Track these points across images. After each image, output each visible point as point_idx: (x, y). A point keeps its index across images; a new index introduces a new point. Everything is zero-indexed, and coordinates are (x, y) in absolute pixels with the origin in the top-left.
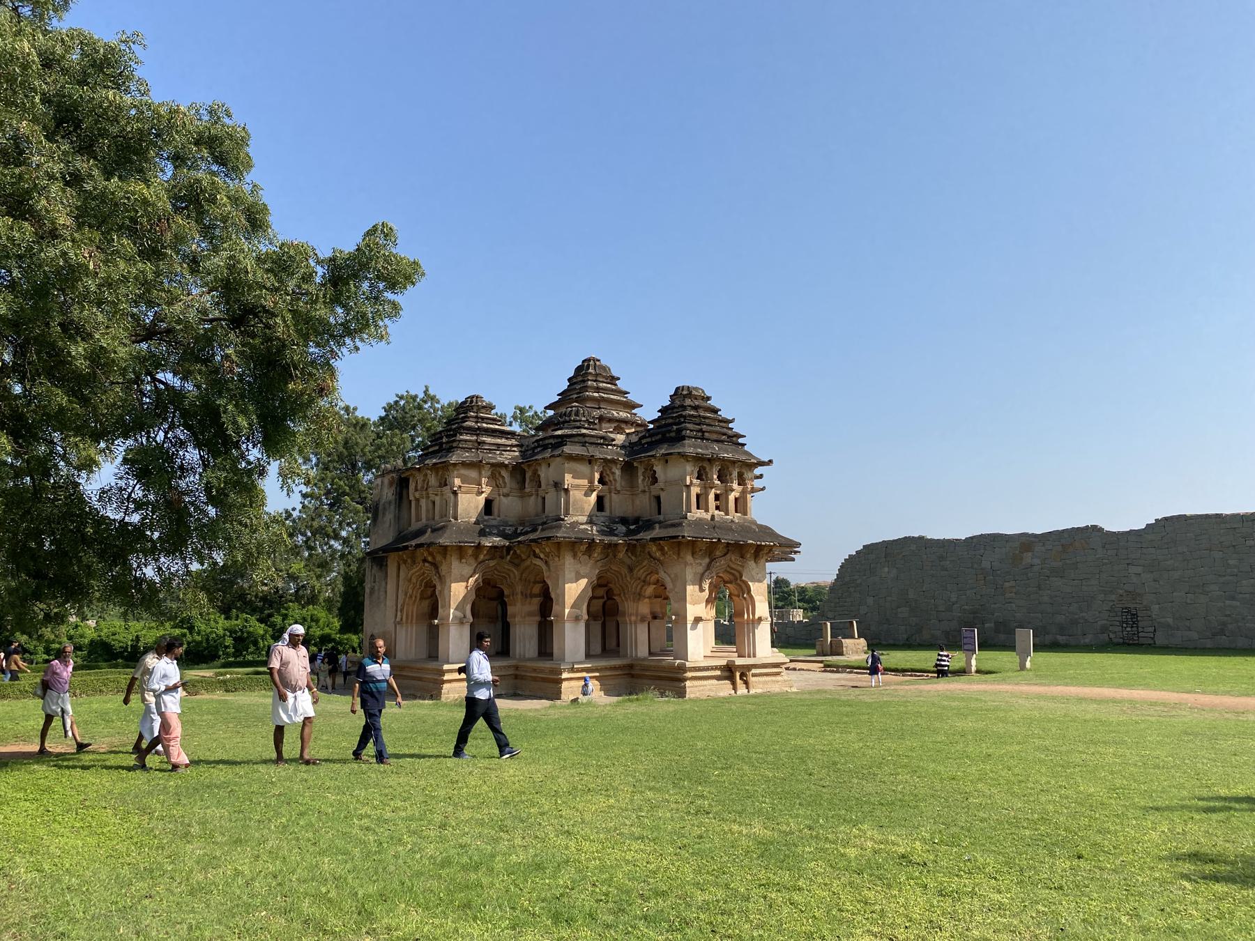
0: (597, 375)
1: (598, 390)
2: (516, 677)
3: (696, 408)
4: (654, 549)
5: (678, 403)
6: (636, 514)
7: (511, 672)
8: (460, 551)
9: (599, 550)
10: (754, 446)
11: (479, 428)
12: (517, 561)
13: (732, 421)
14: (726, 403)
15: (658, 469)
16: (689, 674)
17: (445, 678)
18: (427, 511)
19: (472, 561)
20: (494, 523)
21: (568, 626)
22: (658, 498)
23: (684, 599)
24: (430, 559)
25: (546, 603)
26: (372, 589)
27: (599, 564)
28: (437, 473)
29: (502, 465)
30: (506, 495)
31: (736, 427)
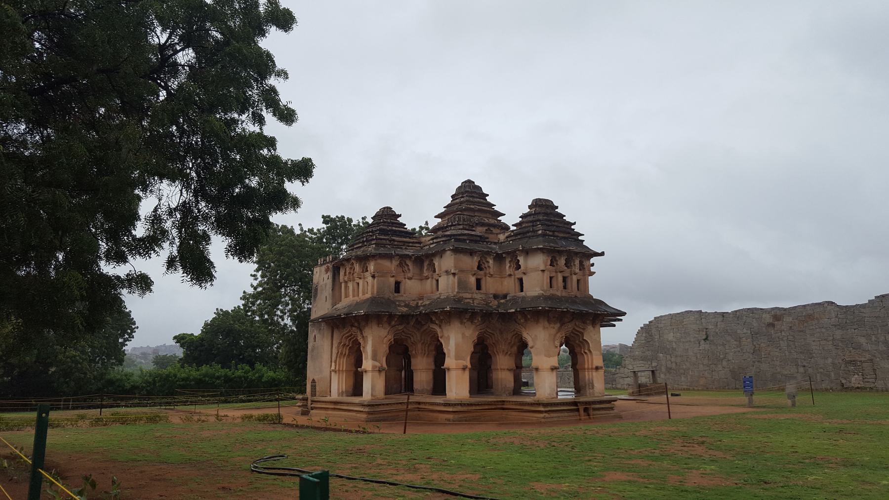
0: (472, 192)
1: (474, 203)
2: (419, 409)
3: (546, 214)
10: (590, 242)
11: (390, 231)
13: (575, 223)
15: (521, 259)
18: (353, 290)
19: (386, 325)
20: (401, 299)
22: (521, 280)
24: (356, 324)
25: (439, 356)
29: (407, 256)
30: (410, 279)
31: (576, 228)
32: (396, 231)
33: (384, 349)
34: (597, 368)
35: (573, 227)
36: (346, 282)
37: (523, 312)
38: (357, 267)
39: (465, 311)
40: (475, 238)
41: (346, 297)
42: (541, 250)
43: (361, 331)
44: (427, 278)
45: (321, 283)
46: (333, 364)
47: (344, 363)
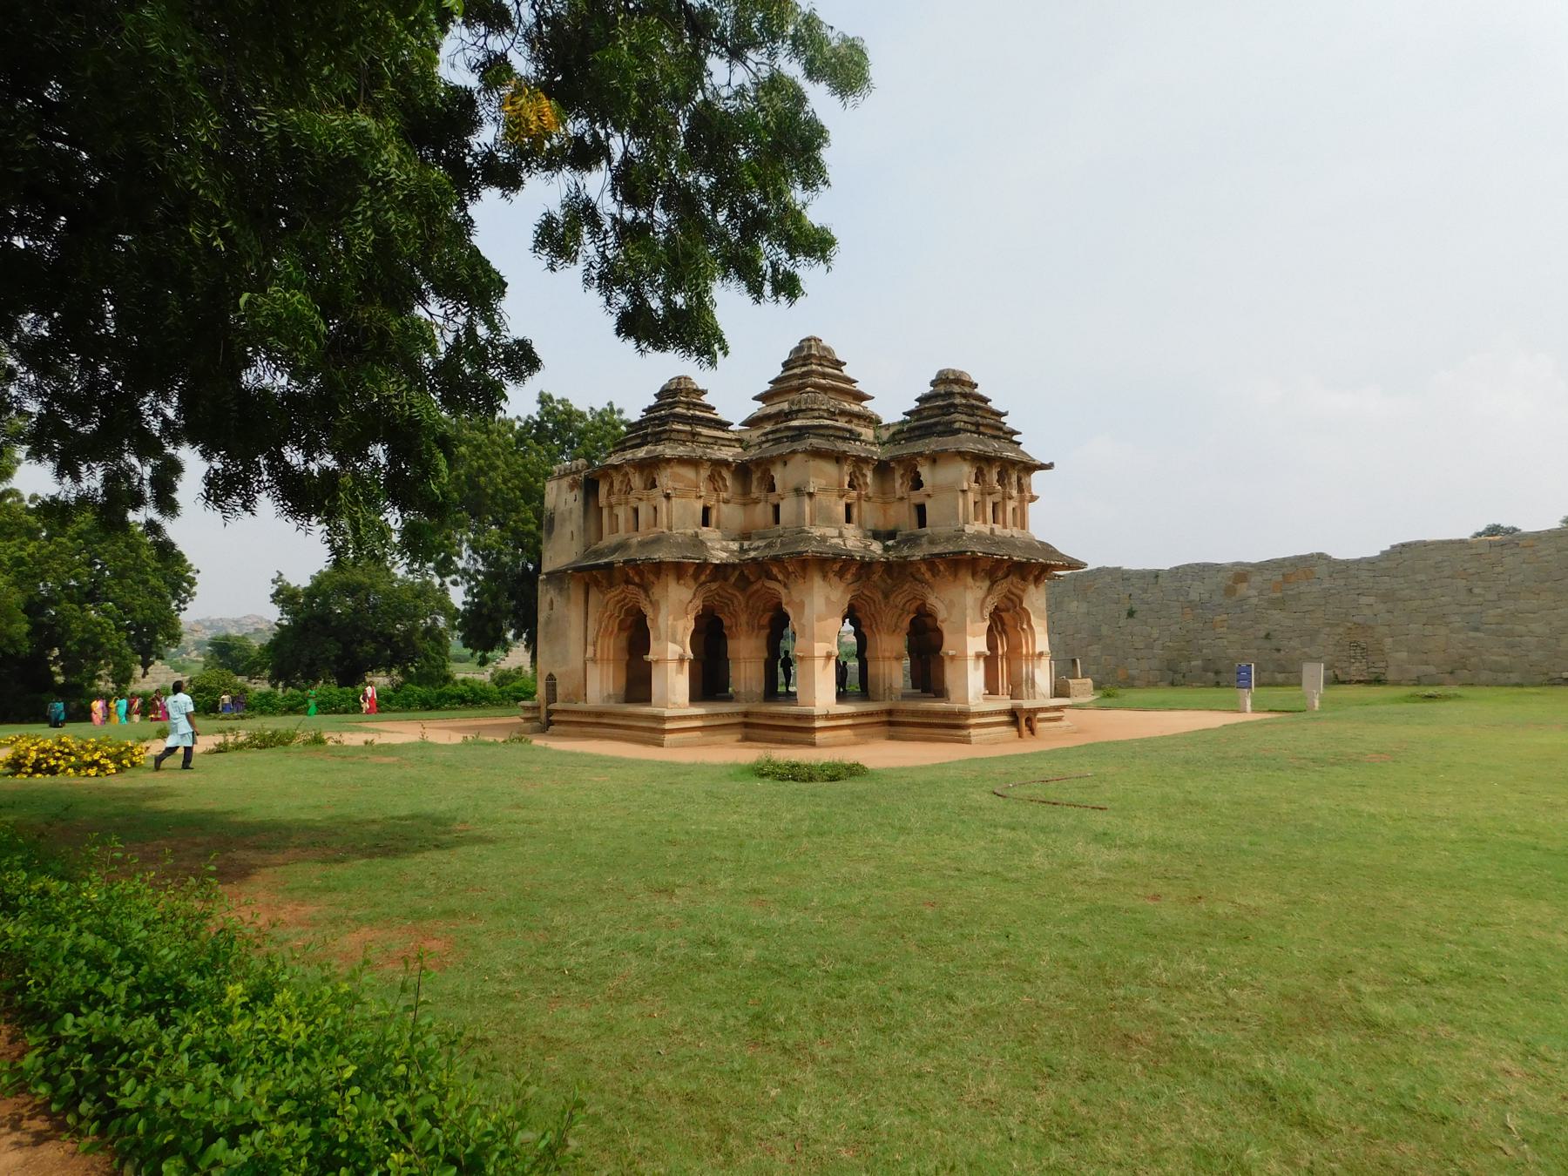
0: (821, 358)
1: (824, 376)
3: (964, 396)
4: (923, 568)
5: (942, 389)
6: (890, 527)
7: (740, 719)
8: (678, 569)
9: (853, 570)
10: (1032, 446)
11: (693, 417)
12: (744, 582)
14: (995, 391)
15: (925, 472)
16: (972, 721)
17: (668, 726)
18: (627, 520)
19: (692, 583)
21: (819, 664)
23: (962, 630)
24: (637, 580)
26: (549, 621)
27: (852, 587)
28: (641, 472)
29: (725, 463)
30: (726, 502)
31: (1010, 422)
32: (701, 419)
33: (686, 626)
34: (1041, 654)
35: (1003, 419)
36: (611, 507)
37: (931, 562)
38: (637, 481)
39: (836, 558)
40: (840, 434)
41: (612, 532)
42: (962, 455)
43: (646, 591)
44: (756, 502)
45: (562, 507)
46: (590, 649)
47: (612, 645)
